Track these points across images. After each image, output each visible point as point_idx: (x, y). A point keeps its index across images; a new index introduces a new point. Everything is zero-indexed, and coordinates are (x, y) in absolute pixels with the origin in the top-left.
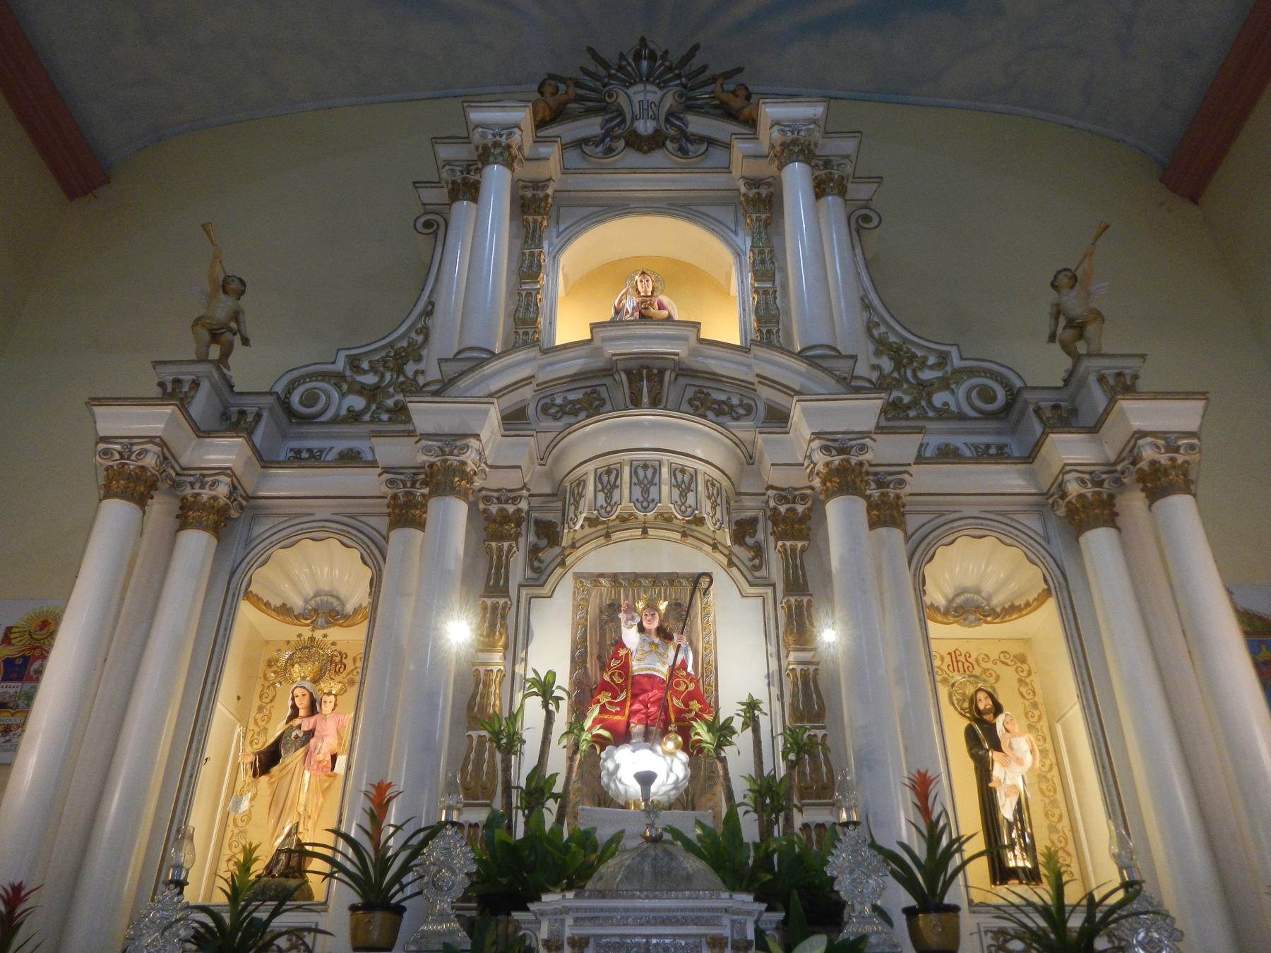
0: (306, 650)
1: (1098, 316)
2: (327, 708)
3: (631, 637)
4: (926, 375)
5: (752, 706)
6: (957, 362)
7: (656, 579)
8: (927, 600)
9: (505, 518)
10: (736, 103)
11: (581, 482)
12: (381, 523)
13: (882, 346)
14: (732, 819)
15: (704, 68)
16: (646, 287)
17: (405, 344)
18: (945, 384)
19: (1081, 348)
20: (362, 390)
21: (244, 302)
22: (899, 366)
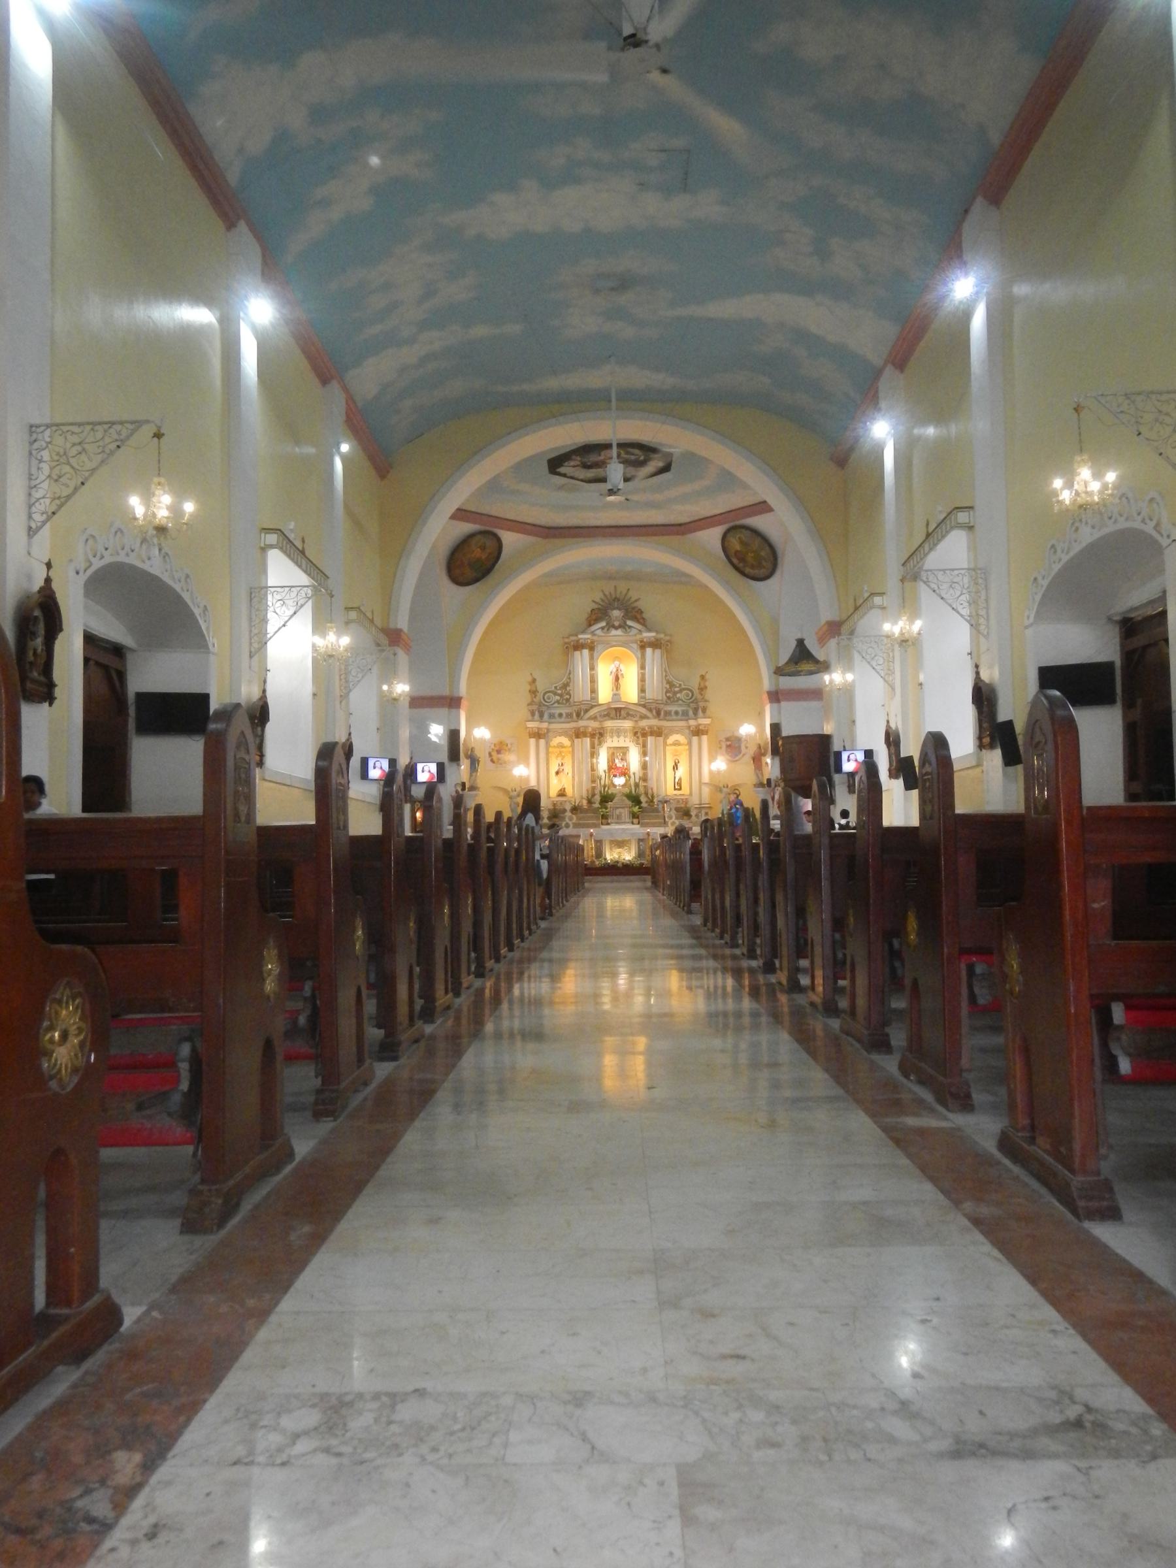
0: (561, 752)
1: (706, 687)
2: (565, 765)
3: (617, 761)
4: (677, 689)
5: (634, 774)
6: (683, 687)
7: (620, 747)
8: (668, 743)
9: (594, 734)
10: (639, 616)
11: (607, 730)
12: (571, 733)
13: (668, 682)
14: (631, 792)
15: (631, 598)
16: (617, 666)
17: (566, 682)
18: (681, 691)
19: (702, 693)
20: (559, 695)
21: (538, 683)
22: (670, 688)
